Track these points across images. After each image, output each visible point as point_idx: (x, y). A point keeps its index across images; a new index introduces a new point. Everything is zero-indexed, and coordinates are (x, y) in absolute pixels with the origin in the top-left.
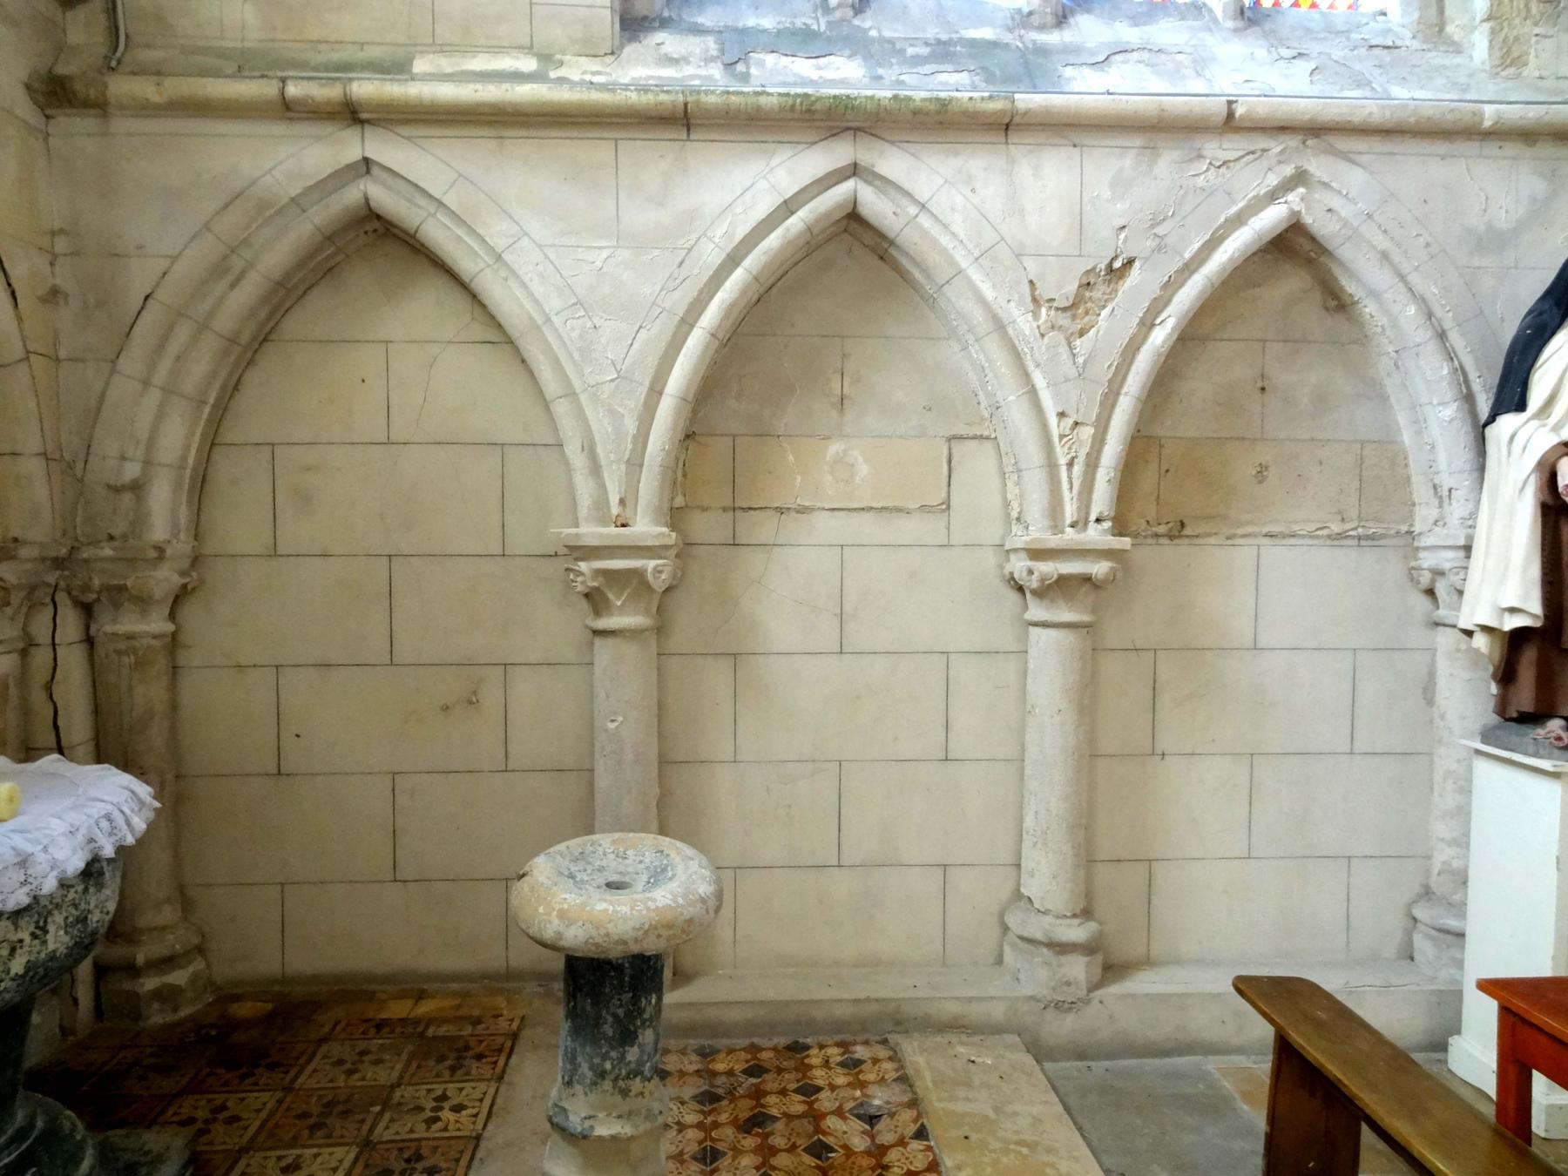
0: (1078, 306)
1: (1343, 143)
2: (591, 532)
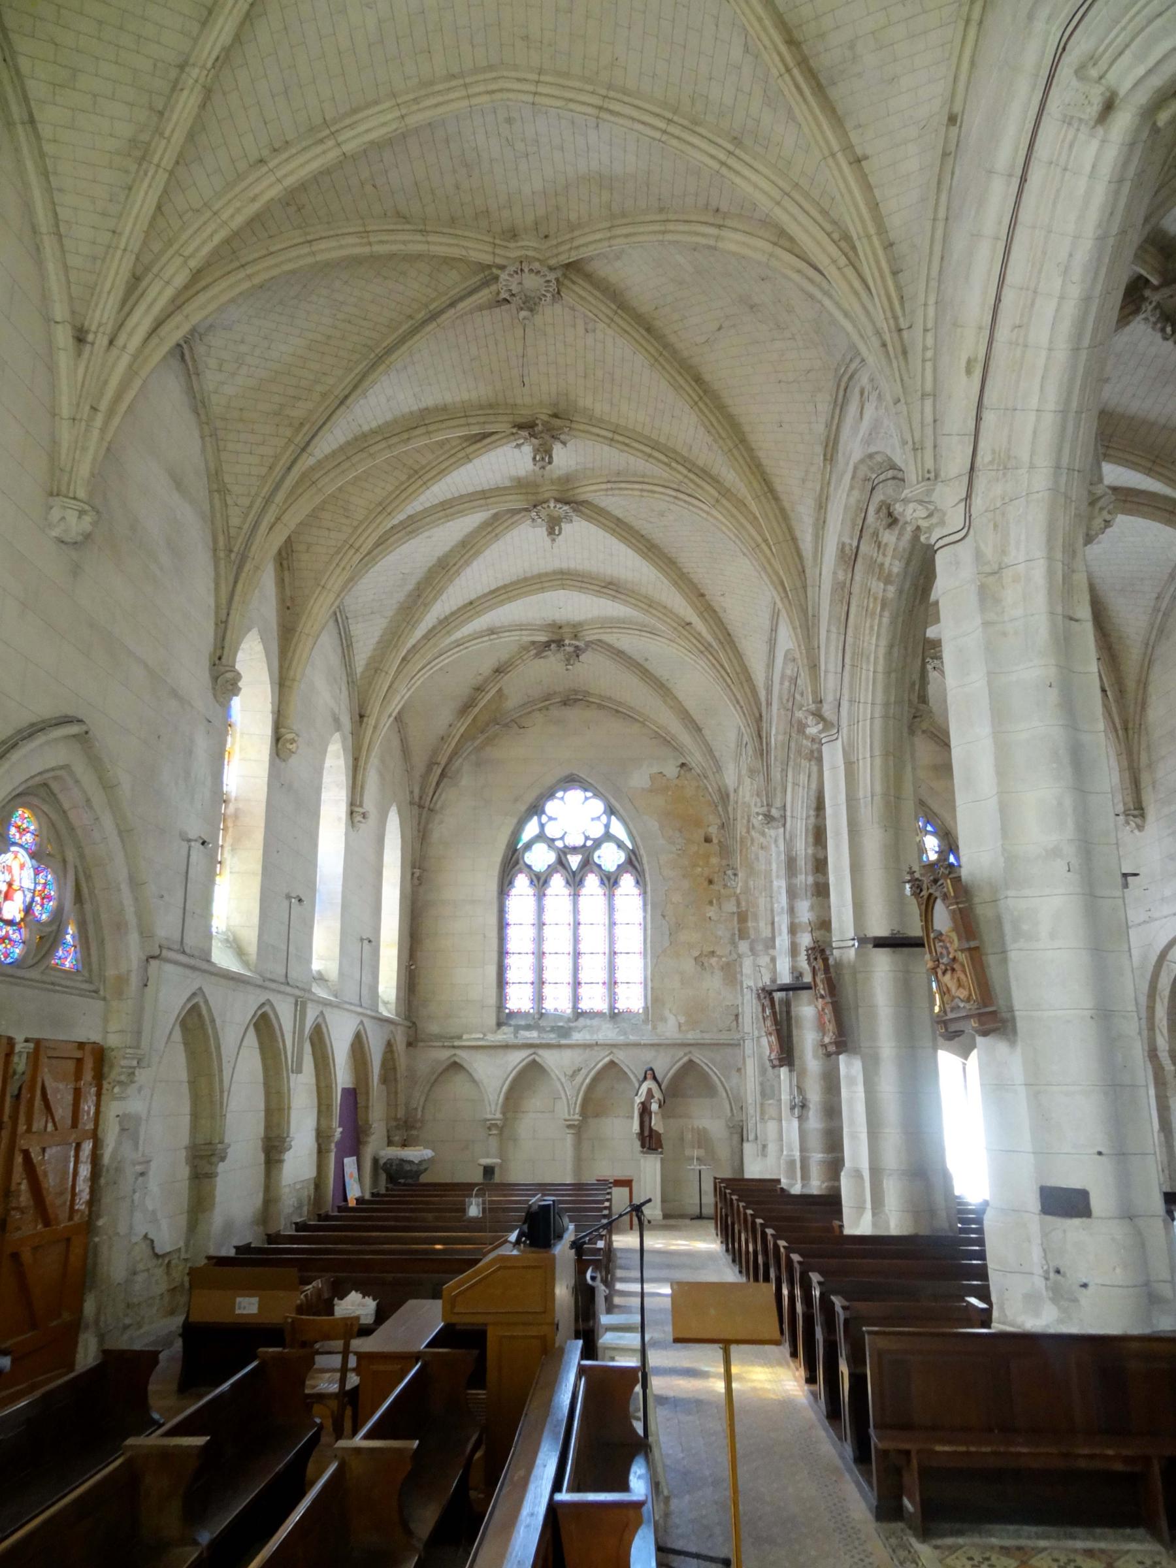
2: (489, 1116)
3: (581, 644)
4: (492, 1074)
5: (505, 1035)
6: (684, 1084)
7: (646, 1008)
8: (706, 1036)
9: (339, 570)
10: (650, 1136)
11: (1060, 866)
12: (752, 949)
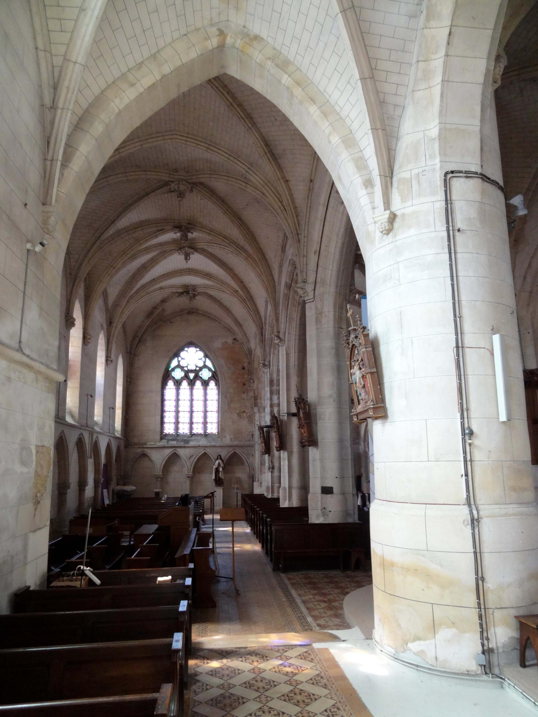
0: (190, 458)
3: (196, 293)
4: (158, 458)
5: (164, 443)
6: (232, 461)
7: (218, 432)
8: (241, 443)
9: (107, 275)
10: (219, 480)
11: (332, 400)
12: (259, 411)
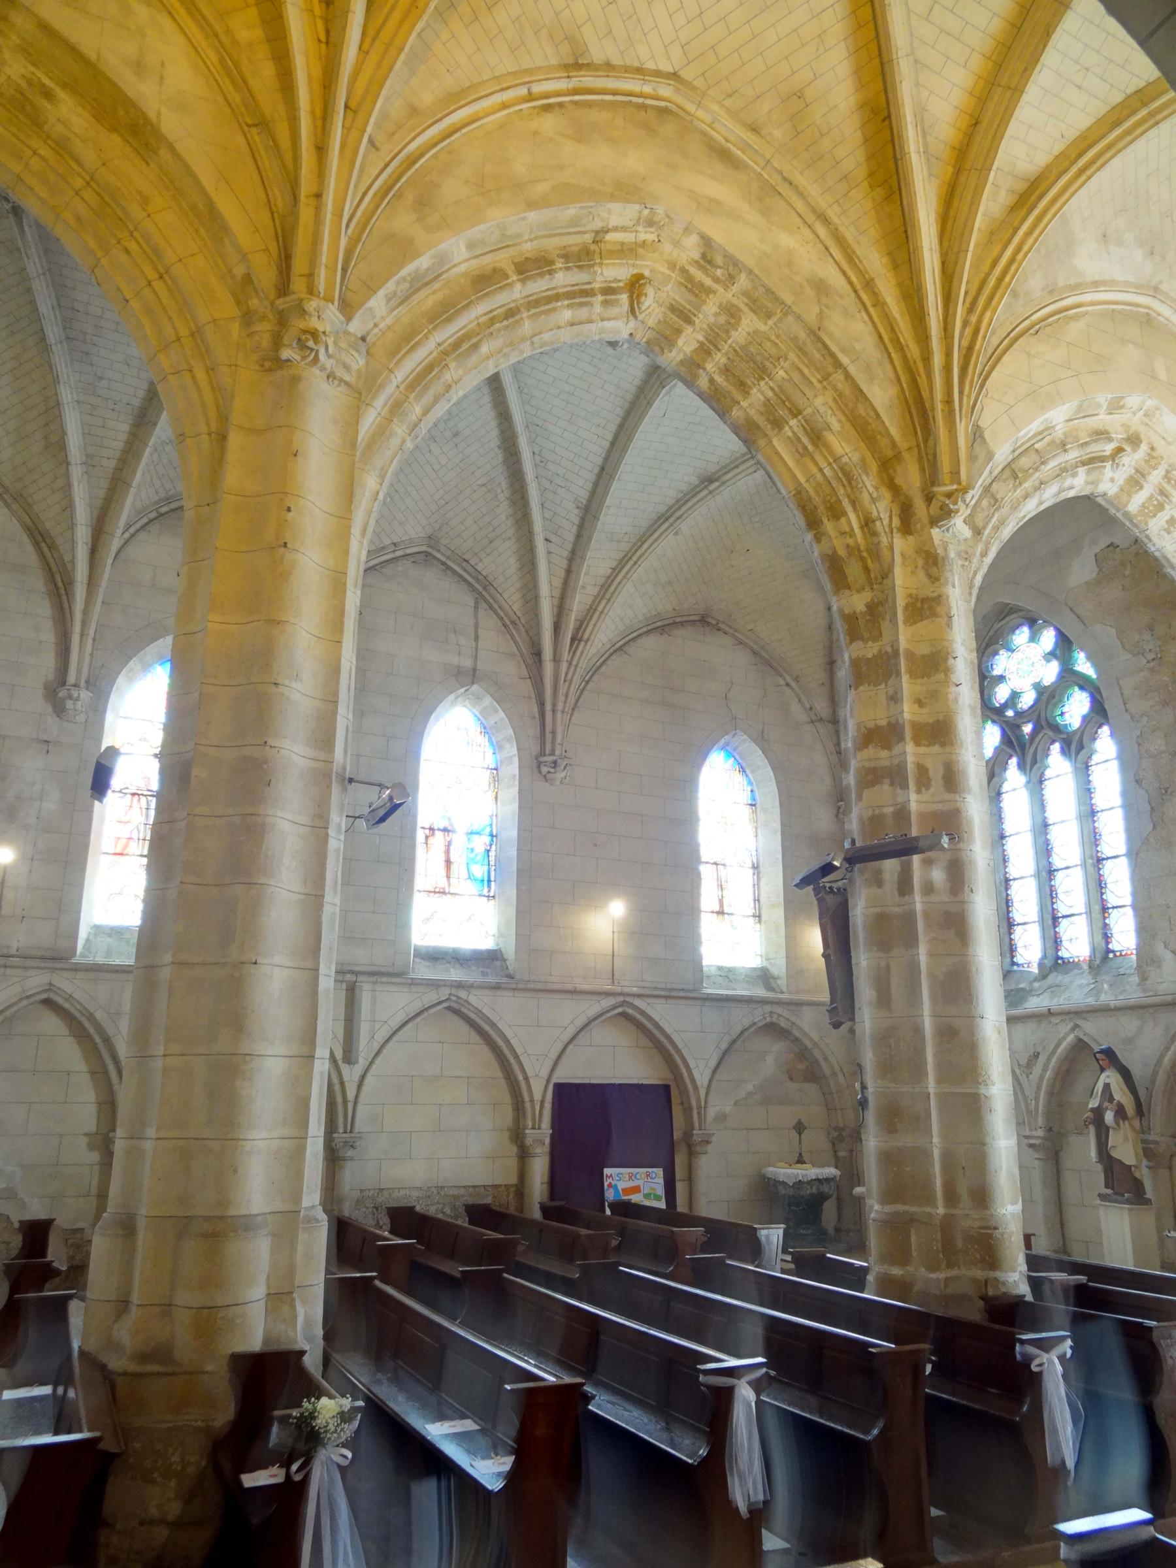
1: (1085, 1015)
